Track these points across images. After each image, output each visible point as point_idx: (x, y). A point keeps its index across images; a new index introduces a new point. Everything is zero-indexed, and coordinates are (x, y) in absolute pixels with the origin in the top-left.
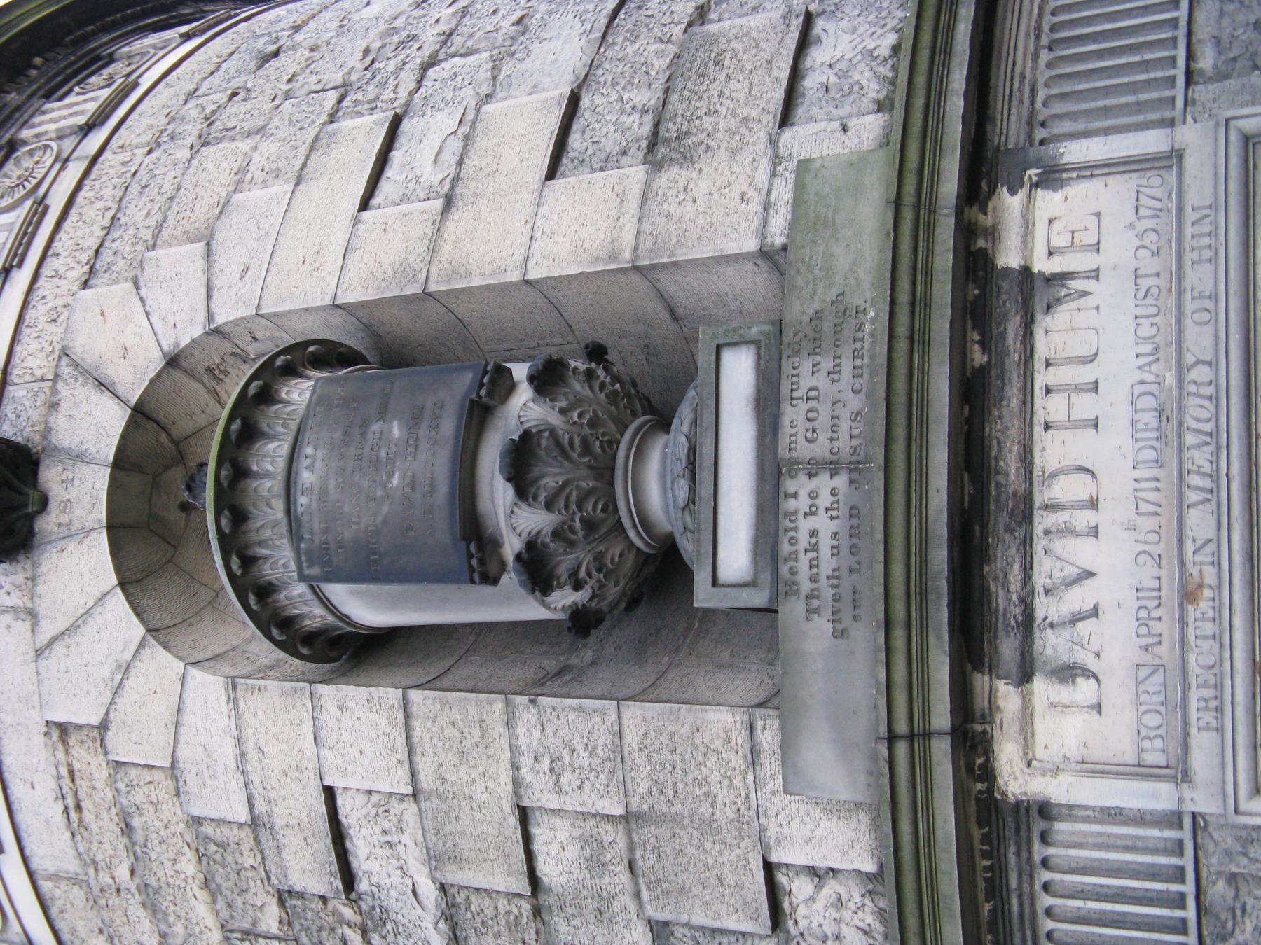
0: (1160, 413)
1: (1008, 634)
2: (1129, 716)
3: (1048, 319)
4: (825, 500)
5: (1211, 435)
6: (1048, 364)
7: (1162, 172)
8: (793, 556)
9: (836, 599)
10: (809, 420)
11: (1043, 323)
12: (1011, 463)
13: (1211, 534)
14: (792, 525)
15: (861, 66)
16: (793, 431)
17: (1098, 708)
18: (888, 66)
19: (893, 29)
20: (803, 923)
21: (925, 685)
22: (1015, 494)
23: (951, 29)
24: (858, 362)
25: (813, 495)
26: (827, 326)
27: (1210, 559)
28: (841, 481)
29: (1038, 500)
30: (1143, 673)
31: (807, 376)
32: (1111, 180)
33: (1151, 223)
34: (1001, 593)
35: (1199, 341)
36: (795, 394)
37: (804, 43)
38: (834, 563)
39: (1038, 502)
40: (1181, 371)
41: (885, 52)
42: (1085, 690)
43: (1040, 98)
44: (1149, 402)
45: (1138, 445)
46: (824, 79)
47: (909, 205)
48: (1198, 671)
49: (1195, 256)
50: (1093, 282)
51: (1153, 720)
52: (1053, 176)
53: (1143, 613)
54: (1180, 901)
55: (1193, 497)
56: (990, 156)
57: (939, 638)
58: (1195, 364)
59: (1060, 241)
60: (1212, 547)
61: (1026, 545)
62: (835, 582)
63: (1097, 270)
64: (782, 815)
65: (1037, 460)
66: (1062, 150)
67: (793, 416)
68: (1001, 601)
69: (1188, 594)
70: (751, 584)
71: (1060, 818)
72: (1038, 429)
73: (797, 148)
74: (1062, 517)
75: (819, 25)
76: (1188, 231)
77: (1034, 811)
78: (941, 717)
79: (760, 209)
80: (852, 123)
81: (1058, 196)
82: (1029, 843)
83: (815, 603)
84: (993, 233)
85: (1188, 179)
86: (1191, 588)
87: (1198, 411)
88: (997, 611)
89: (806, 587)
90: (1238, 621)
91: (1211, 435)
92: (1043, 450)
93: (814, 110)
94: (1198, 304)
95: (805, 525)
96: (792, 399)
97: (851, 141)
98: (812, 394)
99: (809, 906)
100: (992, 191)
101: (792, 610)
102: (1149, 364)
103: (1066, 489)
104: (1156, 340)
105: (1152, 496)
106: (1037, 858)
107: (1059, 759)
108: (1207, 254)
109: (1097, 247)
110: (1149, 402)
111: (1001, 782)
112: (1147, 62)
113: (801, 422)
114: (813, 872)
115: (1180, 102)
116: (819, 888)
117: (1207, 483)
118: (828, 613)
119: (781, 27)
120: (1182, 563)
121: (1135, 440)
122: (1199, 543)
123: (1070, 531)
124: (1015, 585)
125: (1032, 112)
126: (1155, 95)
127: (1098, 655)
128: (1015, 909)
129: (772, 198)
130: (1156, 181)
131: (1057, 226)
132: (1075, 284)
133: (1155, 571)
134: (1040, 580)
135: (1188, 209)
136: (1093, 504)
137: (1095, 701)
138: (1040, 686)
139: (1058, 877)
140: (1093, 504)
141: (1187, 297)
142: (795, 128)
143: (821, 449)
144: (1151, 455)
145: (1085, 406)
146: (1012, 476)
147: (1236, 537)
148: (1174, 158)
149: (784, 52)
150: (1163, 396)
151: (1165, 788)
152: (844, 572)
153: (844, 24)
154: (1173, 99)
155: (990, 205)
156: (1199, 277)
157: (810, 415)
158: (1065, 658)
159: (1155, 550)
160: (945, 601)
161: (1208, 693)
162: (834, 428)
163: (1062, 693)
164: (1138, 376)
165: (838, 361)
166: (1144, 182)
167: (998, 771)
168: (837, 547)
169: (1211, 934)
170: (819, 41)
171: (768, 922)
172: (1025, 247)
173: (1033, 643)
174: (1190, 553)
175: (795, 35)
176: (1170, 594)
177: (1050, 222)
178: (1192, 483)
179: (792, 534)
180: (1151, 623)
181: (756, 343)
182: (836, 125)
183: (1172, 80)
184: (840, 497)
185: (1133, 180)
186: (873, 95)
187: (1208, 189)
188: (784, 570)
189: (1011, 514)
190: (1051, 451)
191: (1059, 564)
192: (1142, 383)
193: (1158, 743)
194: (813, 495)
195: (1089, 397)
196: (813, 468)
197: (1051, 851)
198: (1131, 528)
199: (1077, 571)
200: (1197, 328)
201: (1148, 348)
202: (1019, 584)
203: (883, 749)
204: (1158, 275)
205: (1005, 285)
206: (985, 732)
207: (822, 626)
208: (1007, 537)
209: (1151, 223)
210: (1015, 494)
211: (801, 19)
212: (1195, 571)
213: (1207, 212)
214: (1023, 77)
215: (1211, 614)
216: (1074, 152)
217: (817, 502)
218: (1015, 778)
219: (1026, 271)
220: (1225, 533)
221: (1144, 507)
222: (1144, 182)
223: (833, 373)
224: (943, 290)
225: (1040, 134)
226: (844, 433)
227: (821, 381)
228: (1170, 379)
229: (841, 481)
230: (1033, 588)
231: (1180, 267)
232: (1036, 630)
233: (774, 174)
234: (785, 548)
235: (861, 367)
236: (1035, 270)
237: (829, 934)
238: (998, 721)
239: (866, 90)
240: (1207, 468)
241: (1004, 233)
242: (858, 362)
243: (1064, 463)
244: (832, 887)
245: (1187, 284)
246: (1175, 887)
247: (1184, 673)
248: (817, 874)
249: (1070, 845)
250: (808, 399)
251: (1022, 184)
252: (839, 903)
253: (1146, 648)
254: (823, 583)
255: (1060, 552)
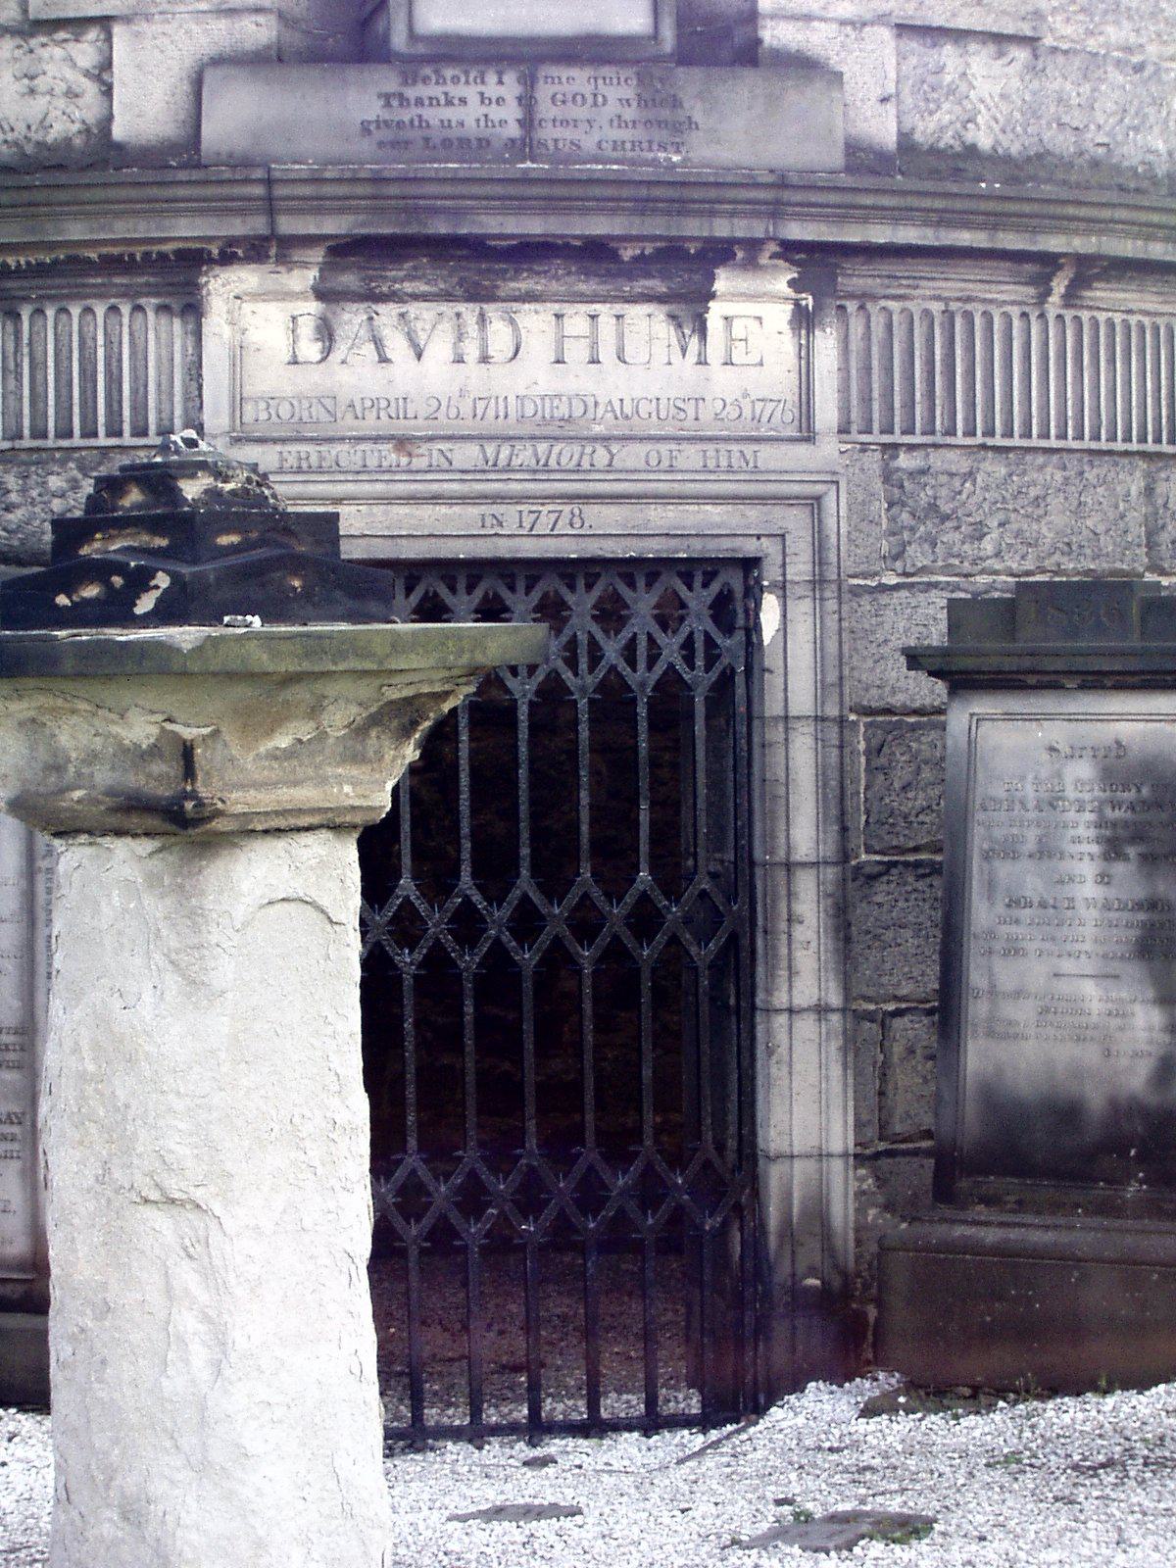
0: (569, 420)
1: (363, 280)
2: (288, 390)
3: (662, 317)
4: (496, 113)
5: (546, 465)
6: (618, 317)
7: (796, 423)
8: (441, 80)
9: (400, 124)
10: (574, 98)
11: (659, 312)
12: (523, 285)
13: (456, 465)
14: (471, 79)
15: (958, 109)
16: (564, 80)
17: (295, 362)
18: (952, 142)
19: (997, 142)
20: (45, 53)
21: (318, 211)
22: (497, 287)
23: (967, 225)
24: (628, 146)
25: (500, 101)
26: (665, 113)
27: (435, 463)
28: (514, 131)
29: (492, 310)
30: (328, 403)
31: (618, 91)
32: (794, 376)
33: (747, 413)
34: (401, 274)
35: (631, 456)
36: (600, 82)
37: (1000, 39)
38: (434, 122)
39: (485, 306)
40: (605, 439)
41: (971, 136)
42: (311, 350)
43: (892, 305)
44: (578, 412)
45: (539, 402)
46: (950, 68)
47: (781, 192)
48: (334, 453)
49: (711, 453)
50: (695, 360)
51: (285, 411)
52: (804, 321)
53: (383, 404)
54: (115, 431)
55: (490, 449)
56: (833, 260)
57: (363, 225)
58: (610, 452)
59: (738, 329)
60: (445, 465)
61: (447, 297)
62: (416, 123)
63: (706, 363)
64: (166, 41)
65: (527, 306)
66: (828, 330)
67: (578, 79)
68: (394, 273)
69: (402, 443)
70: (413, 36)
71: (185, 323)
72: (556, 307)
73: (869, 47)
74: (472, 329)
75: (1021, 54)
76: (735, 447)
77: (189, 300)
78: (288, 225)
79: (805, 11)
80: (891, 108)
81: (786, 328)
82: (157, 295)
83: (395, 103)
84: (751, 264)
85: (784, 447)
86: (409, 447)
87: (567, 454)
88: (384, 269)
89: (411, 93)
90: (379, 488)
91: (546, 465)
92: (536, 312)
93: (913, 60)
94: (665, 454)
95: (471, 92)
96: (596, 79)
97: (871, 108)
98: (600, 99)
99: (64, 62)
100: (793, 262)
101: (387, 79)
102: (613, 411)
103: (500, 335)
104: (636, 417)
105: (491, 413)
106: (142, 301)
107: (243, 324)
108: (711, 464)
109: (729, 363)
110: (578, 412)
111: (217, 270)
112: (913, 407)
113: (569, 89)
114: (107, 65)
115: (864, 438)
116: (87, 74)
117: (502, 462)
118: (386, 115)
119: (1023, 10)
120: (431, 439)
121: (543, 398)
122: (449, 455)
123: (460, 337)
124: (409, 287)
125: (874, 298)
126: (876, 416)
127: (343, 362)
128: (92, 281)
129: (816, 24)
130: (788, 417)
131: (754, 325)
132: (694, 343)
133: (422, 414)
134: (413, 309)
135: (756, 447)
136: (485, 359)
137: (300, 359)
138: (314, 307)
139: (126, 321)
140: (485, 359)
141: (673, 446)
142: (893, 44)
143: (546, 110)
144: (529, 412)
145: (577, 352)
146: (513, 285)
147: (455, 486)
148: (807, 435)
149: (990, 19)
150: (581, 423)
151: (224, 421)
152: (426, 133)
153: (1016, 83)
154: (871, 433)
155: (780, 262)
156: (690, 456)
157: (579, 98)
158: (339, 333)
159: (441, 415)
160: (398, 231)
161: (314, 460)
162: (565, 123)
163: (307, 327)
164: (603, 401)
165: (630, 125)
166: (789, 405)
167: (230, 268)
168: (450, 126)
169: (84, 458)
170: (1001, 54)
171: (44, 16)
172: (734, 295)
173: (355, 302)
174: (440, 446)
175: (1010, 30)
176: (401, 428)
177: (759, 318)
178: (503, 448)
179: (463, 79)
180: (374, 410)
181: (655, 36)
182: (891, 89)
183: (888, 430)
184: (498, 129)
185: (792, 397)
186: (921, 126)
187: (771, 467)
188: (427, 71)
189: (477, 284)
190: (535, 320)
191: (428, 327)
192: (596, 404)
193: (263, 416)
194: (500, 101)
195: (586, 355)
196: (527, 102)
197: (151, 315)
198: (462, 394)
199: (422, 343)
200: (643, 455)
201: (628, 410)
202: (410, 290)
203: (259, 174)
204: (697, 419)
205: (697, 277)
206: (268, 257)
207: (374, 110)
208: (455, 280)
209: (747, 413)
210: (497, 287)
211: (1029, 33)
212: (424, 448)
213: (751, 465)
214: (916, 287)
215: (385, 464)
216: (826, 344)
217: (494, 105)
218: (224, 285)
219: (712, 296)
220: (458, 476)
221: (481, 405)
222: (789, 405)
223: (619, 121)
224: (693, 228)
225: (851, 306)
226: (560, 133)
227: (612, 108)
228: (598, 429)
229: (514, 131)
230: (405, 302)
231: (702, 439)
232: (366, 305)
233: (843, 23)
234: (449, 73)
235: (624, 149)
236: (711, 304)
237: (36, 82)
238: (279, 269)
239: (928, 118)
240: (516, 462)
241: (750, 274)
242: (628, 146)
243: (523, 331)
244: (91, 89)
245: (684, 446)
246: (127, 428)
247: (330, 440)
248: (102, 73)
249: (160, 334)
250: (595, 95)
251: (798, 291)
252: (72, 94)
253: (352, 406)
254: (414, 111)
255: (440, 327)
